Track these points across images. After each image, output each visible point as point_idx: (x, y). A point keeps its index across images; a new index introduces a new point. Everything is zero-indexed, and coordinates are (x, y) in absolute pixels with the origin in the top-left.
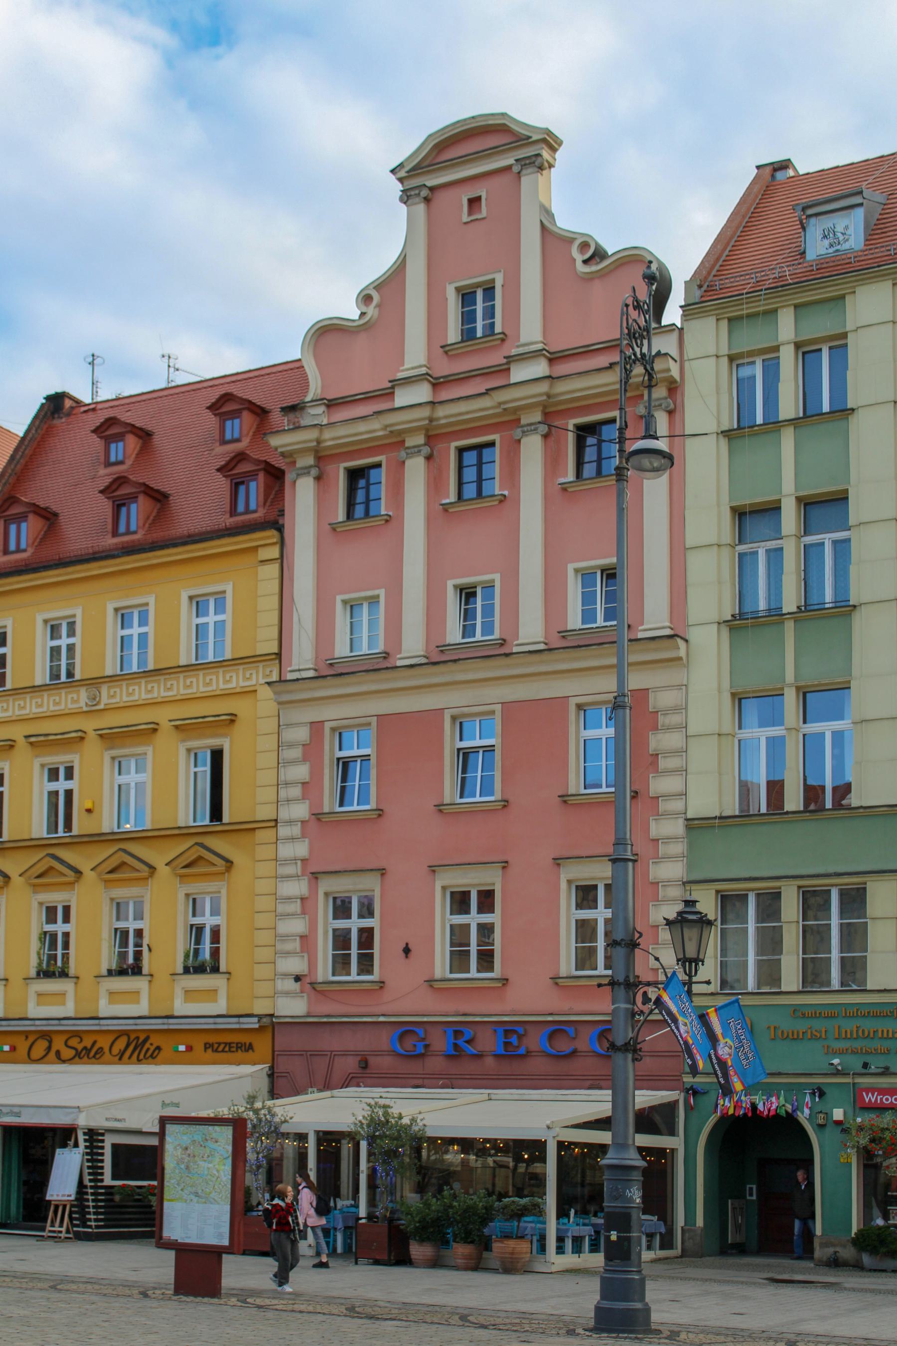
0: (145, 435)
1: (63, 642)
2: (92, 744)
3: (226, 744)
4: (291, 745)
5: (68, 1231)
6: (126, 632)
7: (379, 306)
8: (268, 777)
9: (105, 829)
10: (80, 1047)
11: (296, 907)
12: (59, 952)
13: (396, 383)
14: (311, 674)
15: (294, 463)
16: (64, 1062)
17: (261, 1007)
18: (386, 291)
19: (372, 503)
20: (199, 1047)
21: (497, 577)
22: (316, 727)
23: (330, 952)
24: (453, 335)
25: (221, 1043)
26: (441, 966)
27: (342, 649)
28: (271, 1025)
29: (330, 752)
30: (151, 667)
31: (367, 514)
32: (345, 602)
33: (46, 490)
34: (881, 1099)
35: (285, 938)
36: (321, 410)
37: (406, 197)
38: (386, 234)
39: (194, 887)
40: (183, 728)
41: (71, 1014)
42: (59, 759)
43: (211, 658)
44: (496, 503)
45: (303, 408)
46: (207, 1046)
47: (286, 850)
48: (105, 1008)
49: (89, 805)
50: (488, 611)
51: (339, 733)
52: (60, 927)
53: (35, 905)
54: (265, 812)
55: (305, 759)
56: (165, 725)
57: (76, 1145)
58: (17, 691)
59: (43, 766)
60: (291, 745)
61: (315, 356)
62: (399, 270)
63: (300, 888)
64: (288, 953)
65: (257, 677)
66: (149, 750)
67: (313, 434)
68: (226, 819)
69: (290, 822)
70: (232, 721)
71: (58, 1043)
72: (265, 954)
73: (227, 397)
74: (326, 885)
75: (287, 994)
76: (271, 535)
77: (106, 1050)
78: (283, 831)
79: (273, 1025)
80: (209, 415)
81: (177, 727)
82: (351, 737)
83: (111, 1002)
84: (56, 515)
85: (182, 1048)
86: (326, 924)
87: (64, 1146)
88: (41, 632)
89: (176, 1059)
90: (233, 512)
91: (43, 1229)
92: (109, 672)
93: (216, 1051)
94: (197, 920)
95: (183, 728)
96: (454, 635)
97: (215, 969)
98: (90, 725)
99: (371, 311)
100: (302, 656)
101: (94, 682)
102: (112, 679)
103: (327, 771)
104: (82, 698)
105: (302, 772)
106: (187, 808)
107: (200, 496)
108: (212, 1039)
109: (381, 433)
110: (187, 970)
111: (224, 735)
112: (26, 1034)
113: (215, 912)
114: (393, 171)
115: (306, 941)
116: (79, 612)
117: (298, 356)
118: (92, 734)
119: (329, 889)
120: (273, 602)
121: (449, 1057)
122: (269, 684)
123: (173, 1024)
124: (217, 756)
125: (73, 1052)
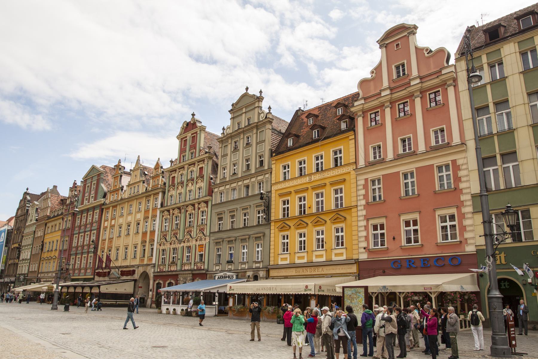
8: (354, 194)
13: (381, 91)
18: (378, 70)
21: (411, 135)
24: (395, 76)
26: (404, 242)
37: (381, 47)
38: (376, 55)
47: (360, 213)
50: (410, 144)
51: (373, 182)
56: (328, 184)
62: (380, 64)
65: (351, 168)
68: (344, 207)
70: (344, 181)
78: (359, 208)
96: (401, 151)
98: (309, 186)
99: (374, 75)
100: (362, 163)
101: (310, 175)
104: (307, 179)
114: (377, 42)
116: (306, 158)
118: (310, 188)
121: (408, 268)
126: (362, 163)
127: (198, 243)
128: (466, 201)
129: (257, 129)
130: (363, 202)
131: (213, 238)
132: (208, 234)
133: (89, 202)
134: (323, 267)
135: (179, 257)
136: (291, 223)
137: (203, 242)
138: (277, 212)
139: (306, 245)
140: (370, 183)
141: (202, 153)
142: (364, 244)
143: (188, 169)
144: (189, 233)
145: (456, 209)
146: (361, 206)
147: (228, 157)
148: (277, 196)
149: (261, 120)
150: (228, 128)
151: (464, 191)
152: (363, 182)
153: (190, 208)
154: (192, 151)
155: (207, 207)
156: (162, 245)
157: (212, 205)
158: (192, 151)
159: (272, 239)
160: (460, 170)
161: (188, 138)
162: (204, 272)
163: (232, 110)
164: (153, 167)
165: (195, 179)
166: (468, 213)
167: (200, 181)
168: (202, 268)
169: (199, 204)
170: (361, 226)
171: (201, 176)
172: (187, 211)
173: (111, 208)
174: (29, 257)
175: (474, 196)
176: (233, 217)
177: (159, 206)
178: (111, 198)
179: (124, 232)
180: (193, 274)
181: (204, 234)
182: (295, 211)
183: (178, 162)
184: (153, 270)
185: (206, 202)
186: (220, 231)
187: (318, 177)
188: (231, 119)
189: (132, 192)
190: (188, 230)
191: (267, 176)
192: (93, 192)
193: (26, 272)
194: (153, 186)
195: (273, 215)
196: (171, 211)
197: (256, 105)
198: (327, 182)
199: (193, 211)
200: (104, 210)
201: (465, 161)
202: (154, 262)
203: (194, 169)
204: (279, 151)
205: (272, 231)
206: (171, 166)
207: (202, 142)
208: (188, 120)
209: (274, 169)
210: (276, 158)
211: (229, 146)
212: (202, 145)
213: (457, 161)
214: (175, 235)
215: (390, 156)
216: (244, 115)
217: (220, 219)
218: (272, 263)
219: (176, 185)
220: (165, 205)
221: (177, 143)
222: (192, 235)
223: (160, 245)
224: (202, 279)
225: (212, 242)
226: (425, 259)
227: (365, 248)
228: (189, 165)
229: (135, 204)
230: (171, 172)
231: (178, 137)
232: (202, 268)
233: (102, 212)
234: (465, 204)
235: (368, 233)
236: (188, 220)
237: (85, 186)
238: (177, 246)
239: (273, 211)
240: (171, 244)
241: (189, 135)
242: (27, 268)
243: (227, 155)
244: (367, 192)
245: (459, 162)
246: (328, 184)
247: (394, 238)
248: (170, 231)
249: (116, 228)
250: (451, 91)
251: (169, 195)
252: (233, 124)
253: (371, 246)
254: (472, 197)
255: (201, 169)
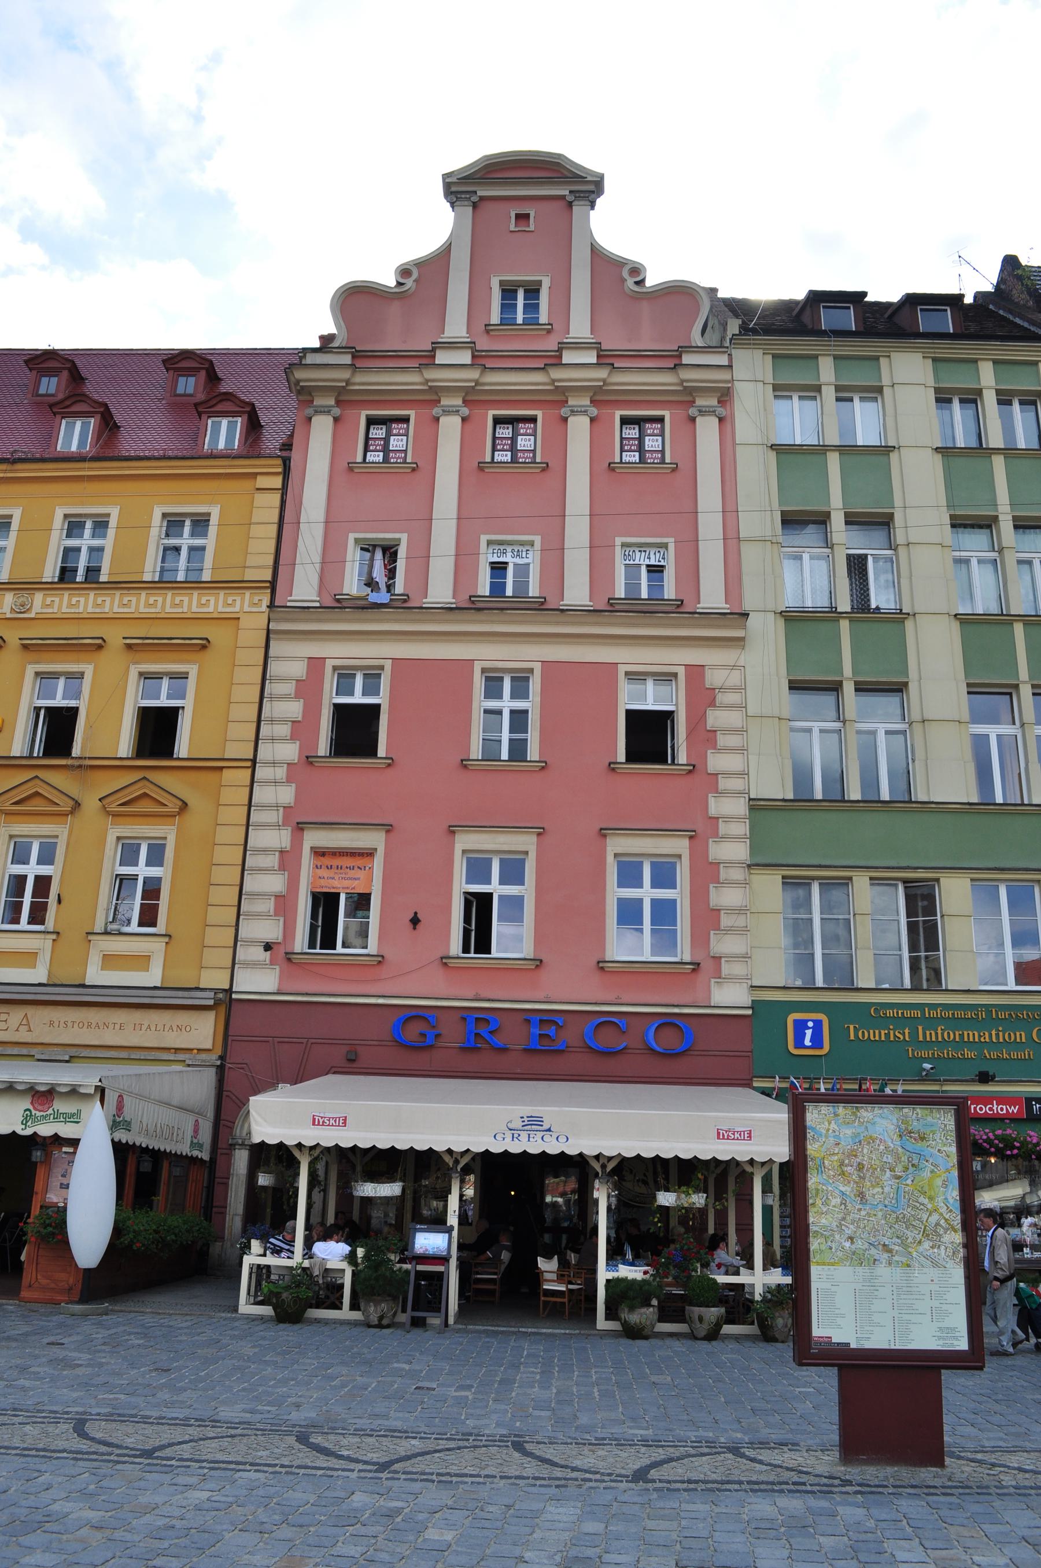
34: (975, 1108)
44: (538, 471)
63: (282, 838)
70: (204, 647)
126: (304, 587)
128: (729, 819)
130: (290, 751)
134: (30, 1011)
140: (330, 682)
145: (686, 842)
146: (274, 763)
151: (723, 783)
152: (299, 670)
160: (712, 704)
166: (730, 864)
170: (265, 851)
175: (757, 807)
187: (64, 603)
198: (115, 636)
201: (735, 678)
213: (708, 673)
215: (440, 590)
226: (547, 1019)
227: (268, 947)
234: (723, 828)
245: (714, 678)
247: (415, 921)
250: (707, 429)
253: (300, 942)
254: (752, 808)
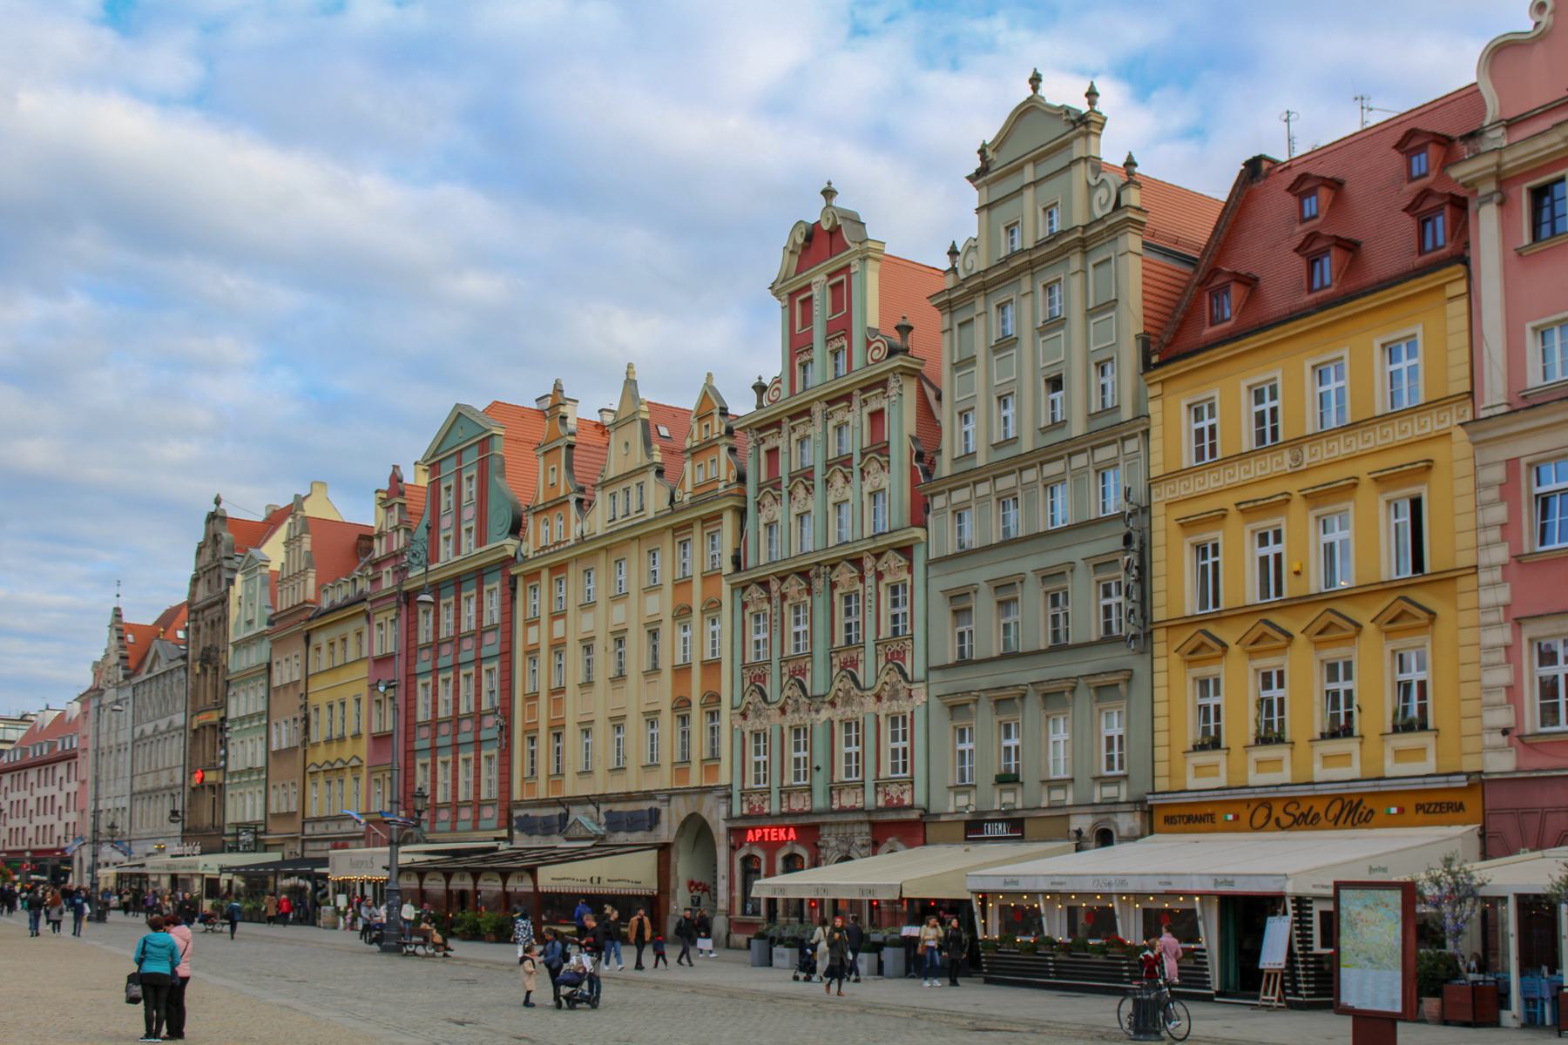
0: (1336, 185)
1: (1267, 406)
2: (1297, 506)
3: (1422, 490)
4: (1487, 486)
5: (1280, 1000)
6: (1394, 367)
7: (1553, 12)
9: (1313, 591)
10: (1297, 813)
11: (1500, 656)
12: (1276, 718)
14: (1504, 409)
15: (1476, 191)
16: (1283, 829)
17: (1470, 764)
19: (1558, 222)
20: (1410, 809)
22: (1512, 464)
23: (1538, 702)
25: (1431, 804)
27: (1534, 379)
28: (1480, 782)
29: (1528, 488)
30: (1349, 421)
31: (1553, 233)
32: (1535, 329)
33: (1248, 258)
35: (1490, 689)
36: (1500, 132)
39: (1399, 643)
40: (1383, 480)
41: (1288, 780)
42: (1267, 524)
43: (1406, 405)
45: (1482, 134)
46: (1419, 807)
47: (1488, 597)
48: (1320, 772)
49: (1296, 567)
51: (1536, 467)
52: (1275, 693)
53: (1251, 672)
54: (1464, 560)
55: (1502, 499)
57: (1285, 913)
58: (1228, 460)
59: (1253, 532)
60: (1487, 486)
61: (1492, 78)
64: (1494, 706)
65: (1450, 419)
66: (1350, 505)
67: (1489, 161)
68: (1427, 569)
69: (1490, 567)
70: (1429, 468)
71: (1277, 811)
72: (1469, 708)
73: (1412, 134)
74: (1529, 631)
75: (1495, 748)
76: (1458, 270)
77: (1322, 815)
78: (1484, 577)
79: (1483, 781)
80: (1395, 153)
81: (1376, 479)
82: (1549, 471)
83: (1324, 766)
84: (1256, 280)
85: (1394, 810)
86: (1533, 672)
87: (1274, 914)
88: (1246, 398)
89: (1390, 822)
90: (1421, 251)
91: (1257, 998)
92: (1309, 431)
93: (1427, 812)
94: (1404, 677)
95: (1383, 480)
97: (1423, 727)
101: (1296, 443)
102: (1313, 438)
103: (1525, 510)
104: (1285, 460)
105: (1499, 513)
106: (1390, 564)
107: (1389, 238)
108: (1423, 800)
109: (1562, 146)
110: (1395, 730)
111: (1422, 483)
112: (1248, 802)
113: (1421, 667)
115: (1512, 691)
116: (1279, 375)
117: (1474, 80)
118: (1296, 496)
119: (1534, 634)
120: (1464, 338)
122: (1462, 425)
123: (1384, 786)
124: (1416, 505)
125: (1291, 819)
127: (885, 707)
129: (1085, 253)
131: (936, 690)
132: (920, 673)
133: (458, 551)
135: (818, 762)
136: (1229, 634)
137: (902, 706)
138: (1176, 589)
139: (1287, 716)
141: (876, 355)
142: (1503, 717)
143: (827, 417)
144: (850, 667)
147: (979, 369)
148: (1174, 526)
149: (1099, 214)
150: (972, 247)
152: (1498, 474)
153: (845, 575)
154: (836, 344)
155: (910, 569)
156: (750, 715)
157: (929, 563)
158: (836, 344)
159: (1160, 694)
161: (815, 291)
162: (914, 815)
163: (980, 173)
164: (690, 403)
165: (857, 458)
167: (875, 465)
168: (907, 801)
169: (878, 556)
171: (879, 449)
172: (833, 585)
173: (545, 574)
174: (260, 763)
176: (1004, 605)
177: (728, 567)
178: (539, 534)
179: (604, 665)
180: (873, 824)
181: (905, 676)
182: (1242, 587)
183: (785, 392)
184: (723, 809)
185: (906, 551)
186: (963, 662)
188: (978, 211)
189: (620, 511)
190: (842, 656)
191: (1131, 445)
192: (469, 513)
193: (259, 817)
194: (696, 487)
195: (1159, 599)
196: (774, 586)
197: (1078, 150)
199: (859, 586)
200: (520, 582)
202: (724, 779)
203: (849, 417)
204: (1170, 345)
205: (1160, 664)
206: (760, 406)
207: (870, 310)
208: (813, 218)
209: (1156, 419)
210: (1160, 374)
211: (979, 324)
212: (873, 321)
214: (797, 677)
216: (1029, 194)
217: (961, 613)
218: (1162, 784)
219: (785, 482)
220: (750, 563)
221: (774, 317)
222: (860, 677)
223: (744, 716)
224: (910, 845)
225: (934, 702)
227: (1505, 732)
228: (830, 403)
229: (635, 560)
230: (760, 430)
231: (775, 290)
232: (907, 801)
233: (514, 589)
235: (1518, 674)
236: (840, 620)
237: (435, 485)
238: (804, 718)
239: (1158, 584)
240: (783, 711)
241: (819, 280)
242: (260, 801)
243: (970, 361)
244: (1514, 512)
246: (1365, 480)
248: (775, 662)
249: (574, 653)
251: (763, 520)
252: (988, 230)
253: (1532, 723)
255: (877, 416)
